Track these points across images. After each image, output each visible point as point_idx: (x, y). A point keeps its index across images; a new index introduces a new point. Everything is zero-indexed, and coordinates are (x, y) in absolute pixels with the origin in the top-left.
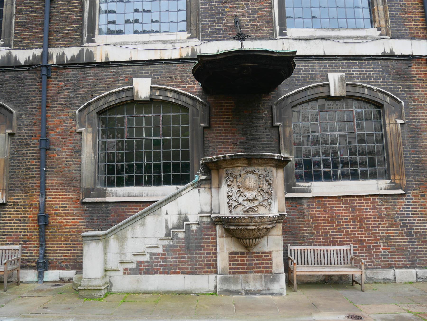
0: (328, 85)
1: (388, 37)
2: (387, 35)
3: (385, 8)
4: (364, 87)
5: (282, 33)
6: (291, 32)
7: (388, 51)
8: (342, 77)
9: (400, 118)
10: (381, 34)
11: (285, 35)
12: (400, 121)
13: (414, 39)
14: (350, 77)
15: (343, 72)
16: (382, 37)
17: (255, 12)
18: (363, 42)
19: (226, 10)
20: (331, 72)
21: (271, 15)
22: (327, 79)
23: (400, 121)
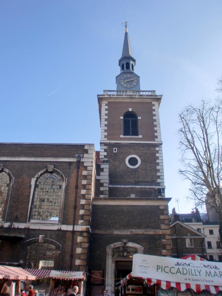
0: (39, 239)
1: (60, 224)
2: (61, 223)
3: (62, 214)
4: (50, 240)
5: (29, 221)
6: (32, 221)
7: (59, 228)
8: (43, 237)
9: (59, 251)
10: (59, 223)
11: (30, 222)
12: (59, 252)
13: (69, 225)
14: (46, 237)
15: (44, 235)
16: (59, 224)
17: (23, 214)
18: (52, 225)
19: (15, 212)
20: (41, 234)
21: (27, 215)
22: (39, 237)
23: (59, 252)
